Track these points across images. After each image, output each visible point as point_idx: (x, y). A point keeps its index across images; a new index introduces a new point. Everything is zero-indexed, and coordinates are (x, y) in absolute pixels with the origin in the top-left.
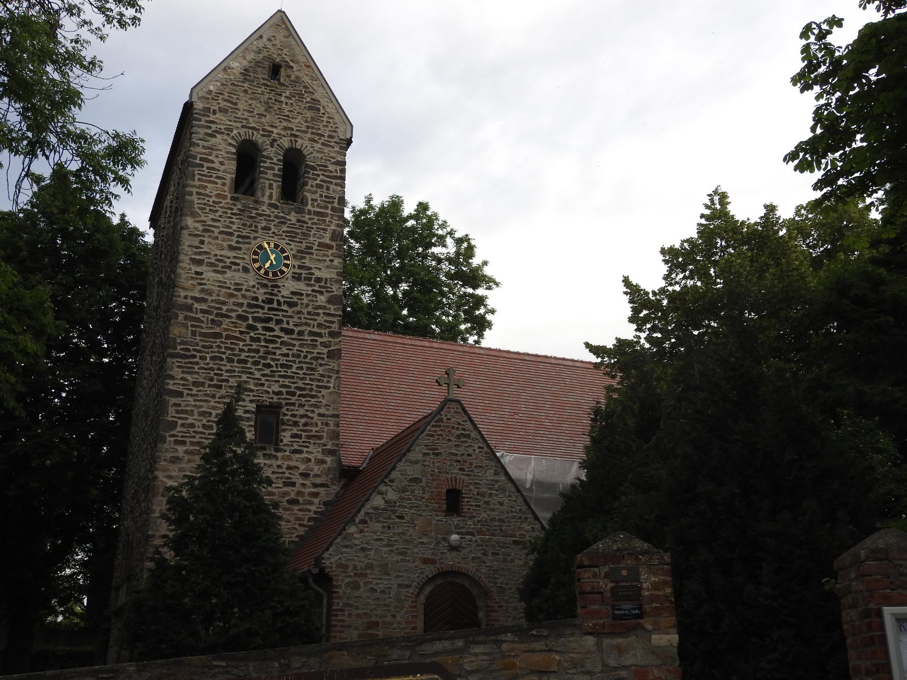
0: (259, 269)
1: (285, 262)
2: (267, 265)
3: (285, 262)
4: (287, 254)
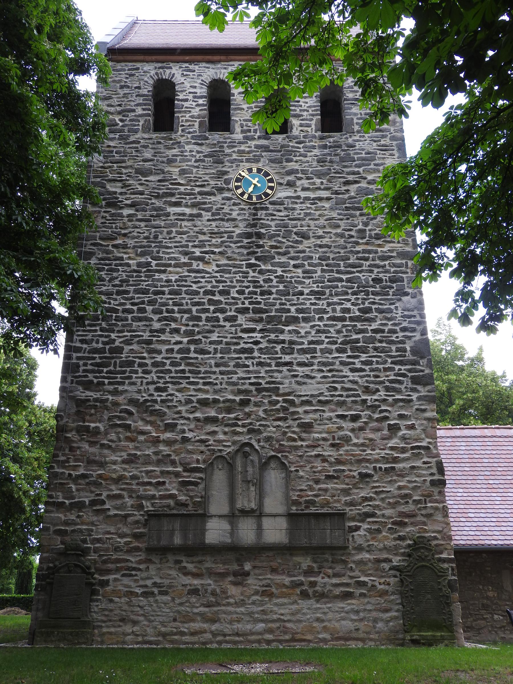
0: (242, 194)
1: (270, 184)
2: (251, 189)
3: (270, 184)
4: (270, 177)
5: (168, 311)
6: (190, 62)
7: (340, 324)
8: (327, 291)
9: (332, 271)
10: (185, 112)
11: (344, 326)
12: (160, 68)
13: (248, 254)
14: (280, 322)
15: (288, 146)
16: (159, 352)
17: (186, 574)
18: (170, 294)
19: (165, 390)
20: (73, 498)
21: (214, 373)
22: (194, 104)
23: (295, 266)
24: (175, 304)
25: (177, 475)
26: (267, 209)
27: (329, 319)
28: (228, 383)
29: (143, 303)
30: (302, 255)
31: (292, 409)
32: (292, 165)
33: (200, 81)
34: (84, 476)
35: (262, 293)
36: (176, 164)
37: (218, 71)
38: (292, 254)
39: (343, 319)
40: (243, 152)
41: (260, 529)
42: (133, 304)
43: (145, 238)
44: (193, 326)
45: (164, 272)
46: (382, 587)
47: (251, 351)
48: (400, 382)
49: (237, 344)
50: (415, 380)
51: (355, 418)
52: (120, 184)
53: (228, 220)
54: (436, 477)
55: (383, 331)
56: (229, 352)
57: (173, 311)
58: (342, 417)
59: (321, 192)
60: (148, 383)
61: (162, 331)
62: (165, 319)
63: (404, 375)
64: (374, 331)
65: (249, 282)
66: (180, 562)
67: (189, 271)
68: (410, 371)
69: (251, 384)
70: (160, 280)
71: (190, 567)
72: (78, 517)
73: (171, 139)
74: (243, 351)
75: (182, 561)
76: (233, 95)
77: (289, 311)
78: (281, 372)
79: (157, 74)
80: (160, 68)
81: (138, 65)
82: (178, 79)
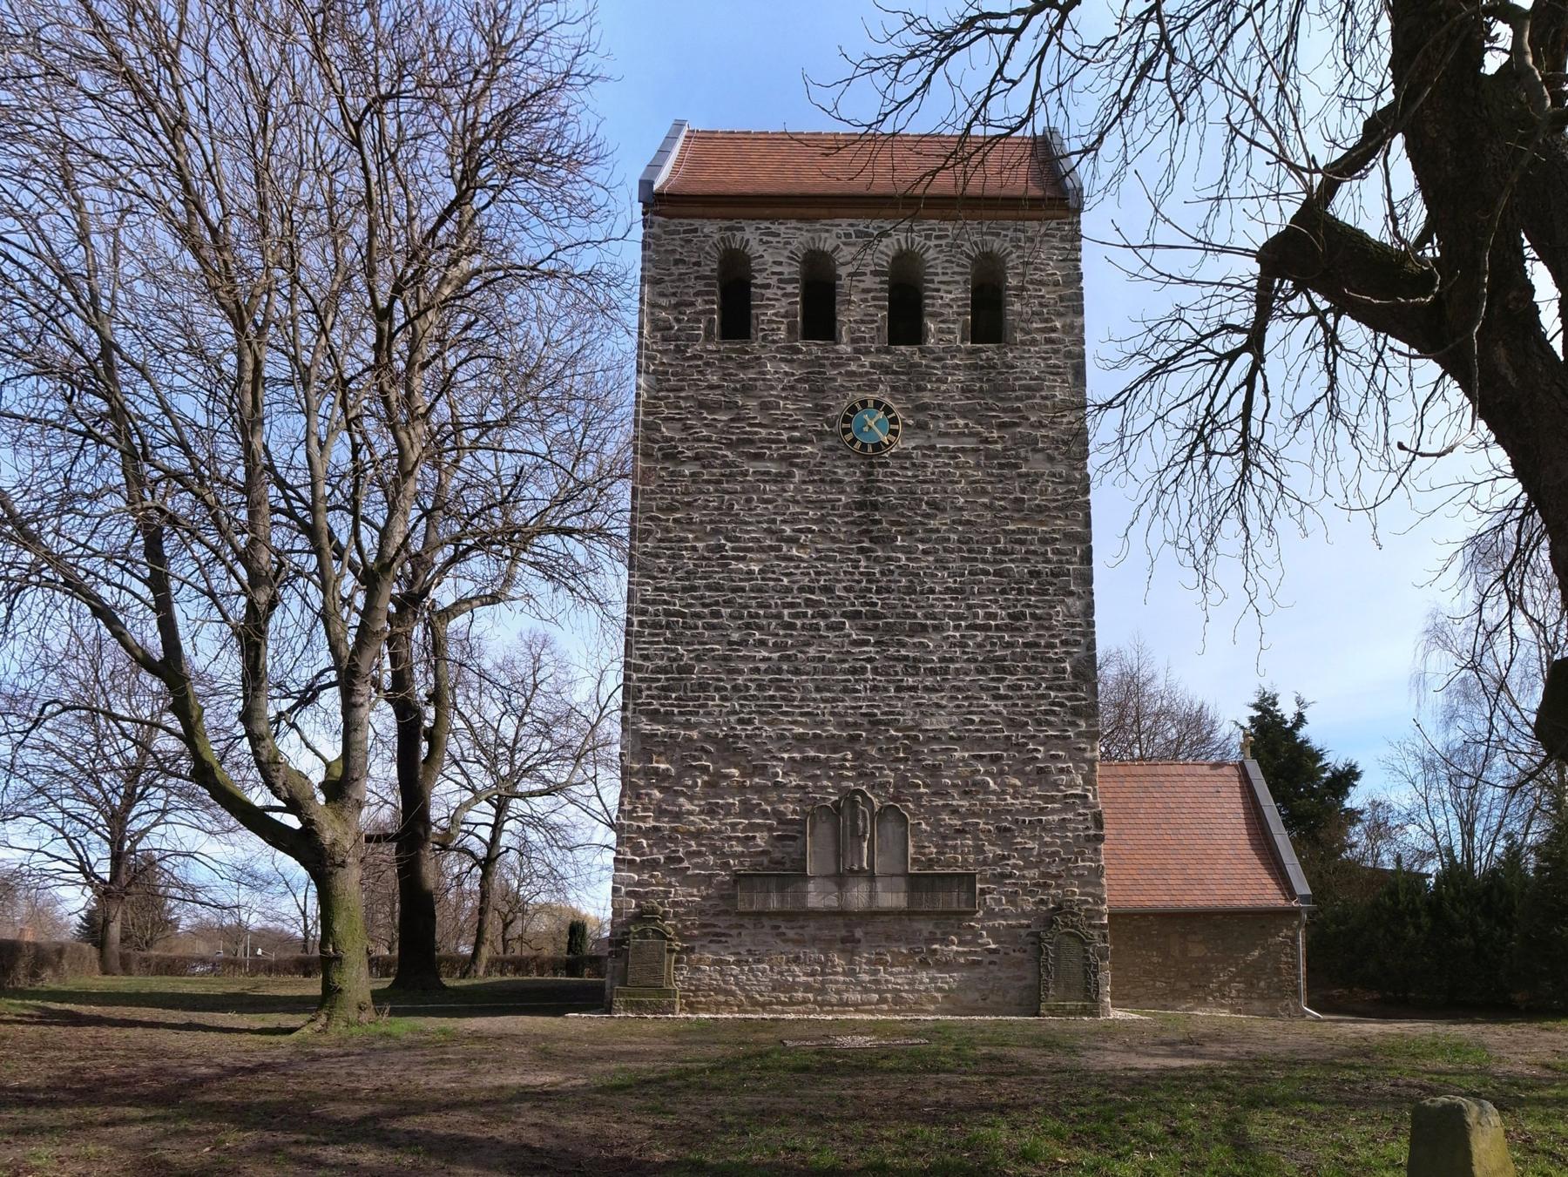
5: (750, 615)
6: (773, 219)
7: (980, 636)
8: (968, 588)
9: (975, 559)
10: (767, 306)
11: (987, 637)
12: (727, 229)
13: (861, 533)
14: (902, 632)
15: (920, 365)
16: (741, 672)
17: (785, 941)
18: (752, 590)
19: (750, 722)
20: (643, 854)
21: (815, 700)
22: (780, 292)
23: (925, 552)
24: (760, 606)
25: (770, 828)
26: (886, 465)
27: (968, 627)
28: (832, 714)
29: (717, 603)
30: (934, 536)
31: (916, 748)
32: (927, 398)
33: (786, 253)
34: (656, 829)
35: (878, 592)
36: (757, 393)
37: (816, 236)
38: (920, 535)
39: (986, 628)
40: (853, 374)
41: (872, 895)
42: (704, 605)
43: (716, 509)
44: (785, 636)
45: (743, 559)
46: (1017, 954)
47: (864, 670)
48: (1054, 713)
49: (844, 661)
50: (1076, 712)
51: (995, 759)
52: (679, 425)
53: (832, 482)
54: (1092, 832)
55: (1037, 645)
56: (833, 672)
57: (757, 616)
58: (980, 758)
59: (965, 439)
60: (729, 713)
61: (743, 643)
62: (748, 626)
63: (1061, 705)
64: (1026, 645)
65: (861, 574)
66: (778, 927)
67: (777, 558)
68: (1069, 699)
69: (863, 715)
70: (740, 571)
71: (791, 934)
72: (652, 876)
73: (747, 353)
74: (853, 671)
75: (778, 927)
76: (840, 278)
77: (915, 616)
78: (902, 699)
79: (722, 239)
80: (727, 229)
81: (697, 223)
82: (755, 248)
